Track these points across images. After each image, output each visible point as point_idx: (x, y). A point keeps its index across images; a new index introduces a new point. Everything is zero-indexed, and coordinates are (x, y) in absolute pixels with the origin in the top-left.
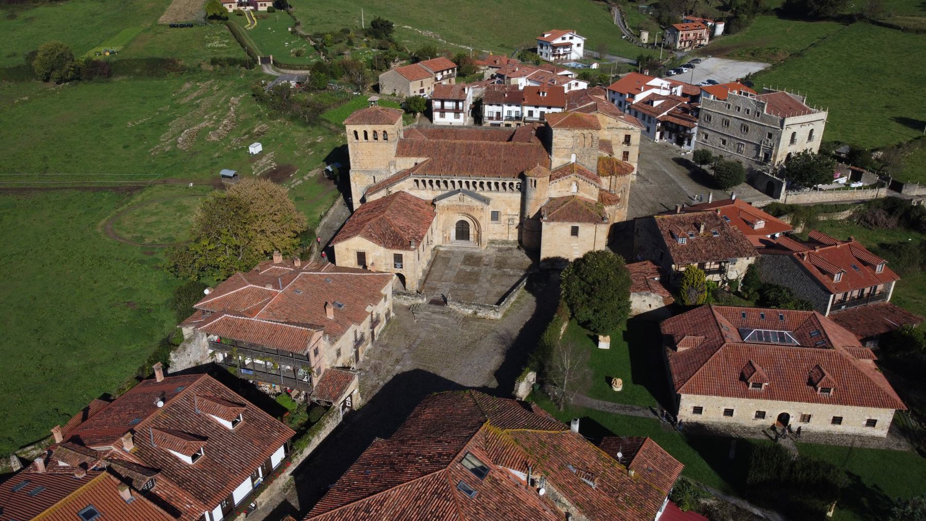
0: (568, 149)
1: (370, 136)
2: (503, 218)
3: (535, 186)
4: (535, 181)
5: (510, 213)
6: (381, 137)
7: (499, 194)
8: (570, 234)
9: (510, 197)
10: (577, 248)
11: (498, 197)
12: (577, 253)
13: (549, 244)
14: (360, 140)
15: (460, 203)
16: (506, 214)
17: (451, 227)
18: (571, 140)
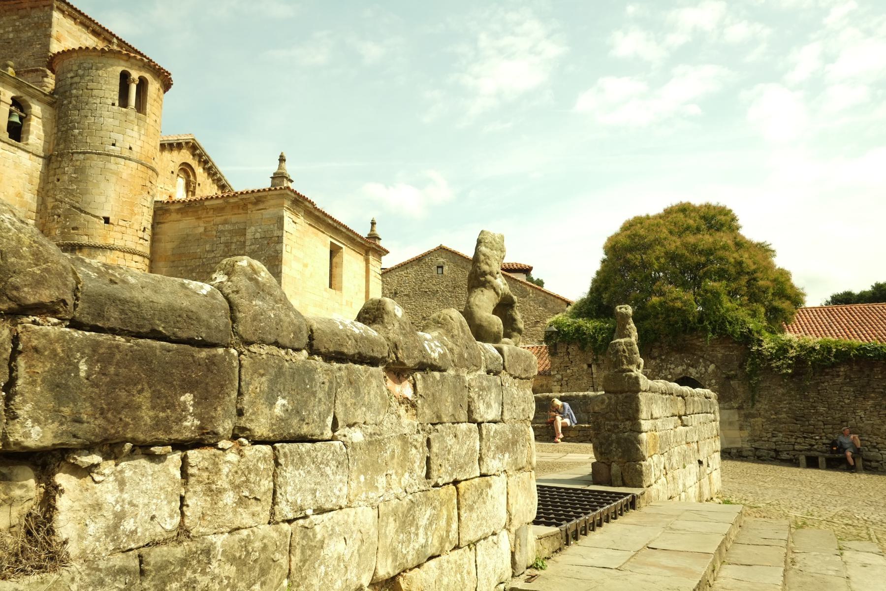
3: (141, 106)
4: (142, 85)
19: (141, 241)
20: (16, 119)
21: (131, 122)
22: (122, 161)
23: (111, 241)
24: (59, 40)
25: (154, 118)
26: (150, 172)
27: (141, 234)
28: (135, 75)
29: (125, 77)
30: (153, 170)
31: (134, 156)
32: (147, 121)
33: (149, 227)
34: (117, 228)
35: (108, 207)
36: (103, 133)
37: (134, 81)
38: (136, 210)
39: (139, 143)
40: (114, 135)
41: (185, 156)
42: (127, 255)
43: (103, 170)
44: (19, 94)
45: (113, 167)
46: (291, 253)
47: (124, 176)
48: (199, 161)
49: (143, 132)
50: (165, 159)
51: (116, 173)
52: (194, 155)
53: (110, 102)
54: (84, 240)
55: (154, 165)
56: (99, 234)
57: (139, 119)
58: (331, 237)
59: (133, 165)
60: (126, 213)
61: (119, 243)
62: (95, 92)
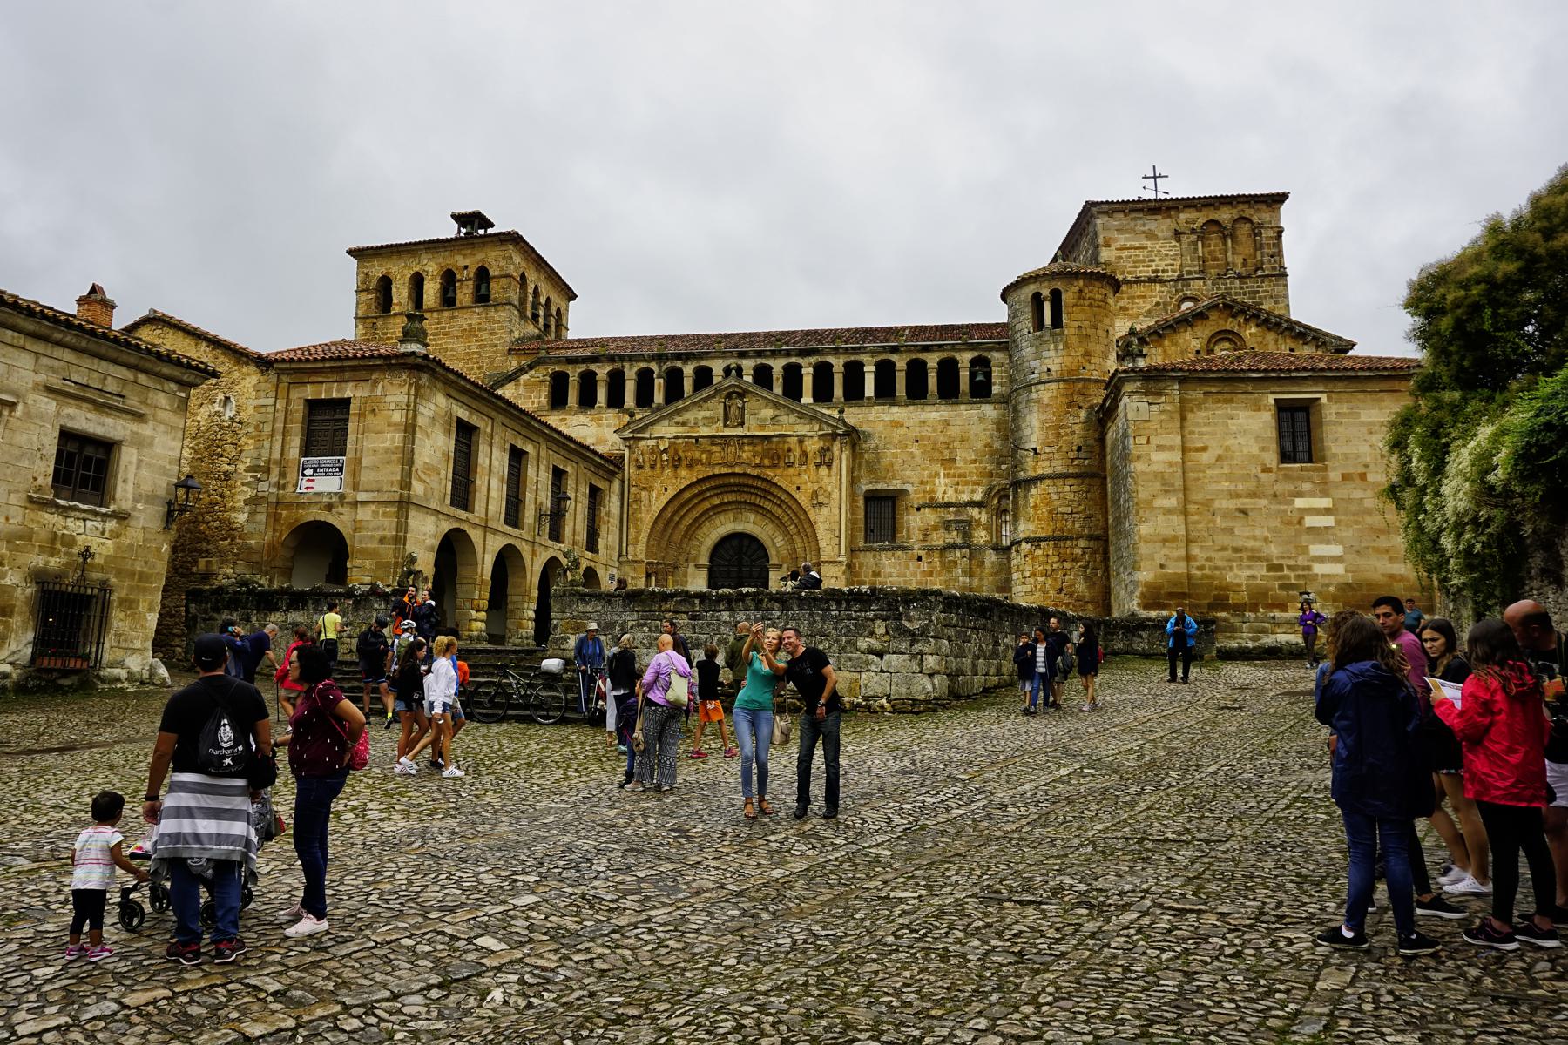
0: (1162, 282)
1: (431, 290)
2: (915, 522)
3: (1057, 322)
4: (1056, 296)
5: (951, 496)
6: (465, 294)
7: (897, 412)
8: (1271, 458)
9: (947, 423)
10: (1329, 521)
11: (897, 424)
12: (1336, 550)
13: (1172, 502)
14: (396, 309)
15: (728, 432)
16: (933, 505)
17: (691, 569)
18: (1172, 248)
19: (1076, 462)
20: (980, 378)
21: (1045, 342)
22: (1041, 387)
23: (1040, 471)
24: (1107, 245)
25: (1076, 324)
26: (1080, 385)
27: (1072, 455)
28: (1046, 292)
29: (1037, 299)
30: (1085, 380)
31: (1054, 376)
32: (1066, 332)
33: (1091, 442)
34: (1043, 457)
35: (1034, 438)
36: (1026, 365)
37: (1045, 299)
38: (1062, 432)
39: (1058, 360)
40: (1033, 363)
41: (1217, 323)
42: (1060, 482)
43: (1028, 401)
44: (976, 354)
45: (1034, 396)
46: (1148, 442)
47: (1046, 401)
48: (1246, 320)
49: (1061, 347)
50: (1181, 341)
51: (1038, 401)
52: (1234, 316)
53: (1026, 332)
54: (1022, 475)
55: (1085, 374)
56: (1033, 467)
57: (1053, 335)
58: (1272, 393)
59: (1053, 386)
60: (1051, 438)
61: (1048, 471)
62: (1018, 327)
